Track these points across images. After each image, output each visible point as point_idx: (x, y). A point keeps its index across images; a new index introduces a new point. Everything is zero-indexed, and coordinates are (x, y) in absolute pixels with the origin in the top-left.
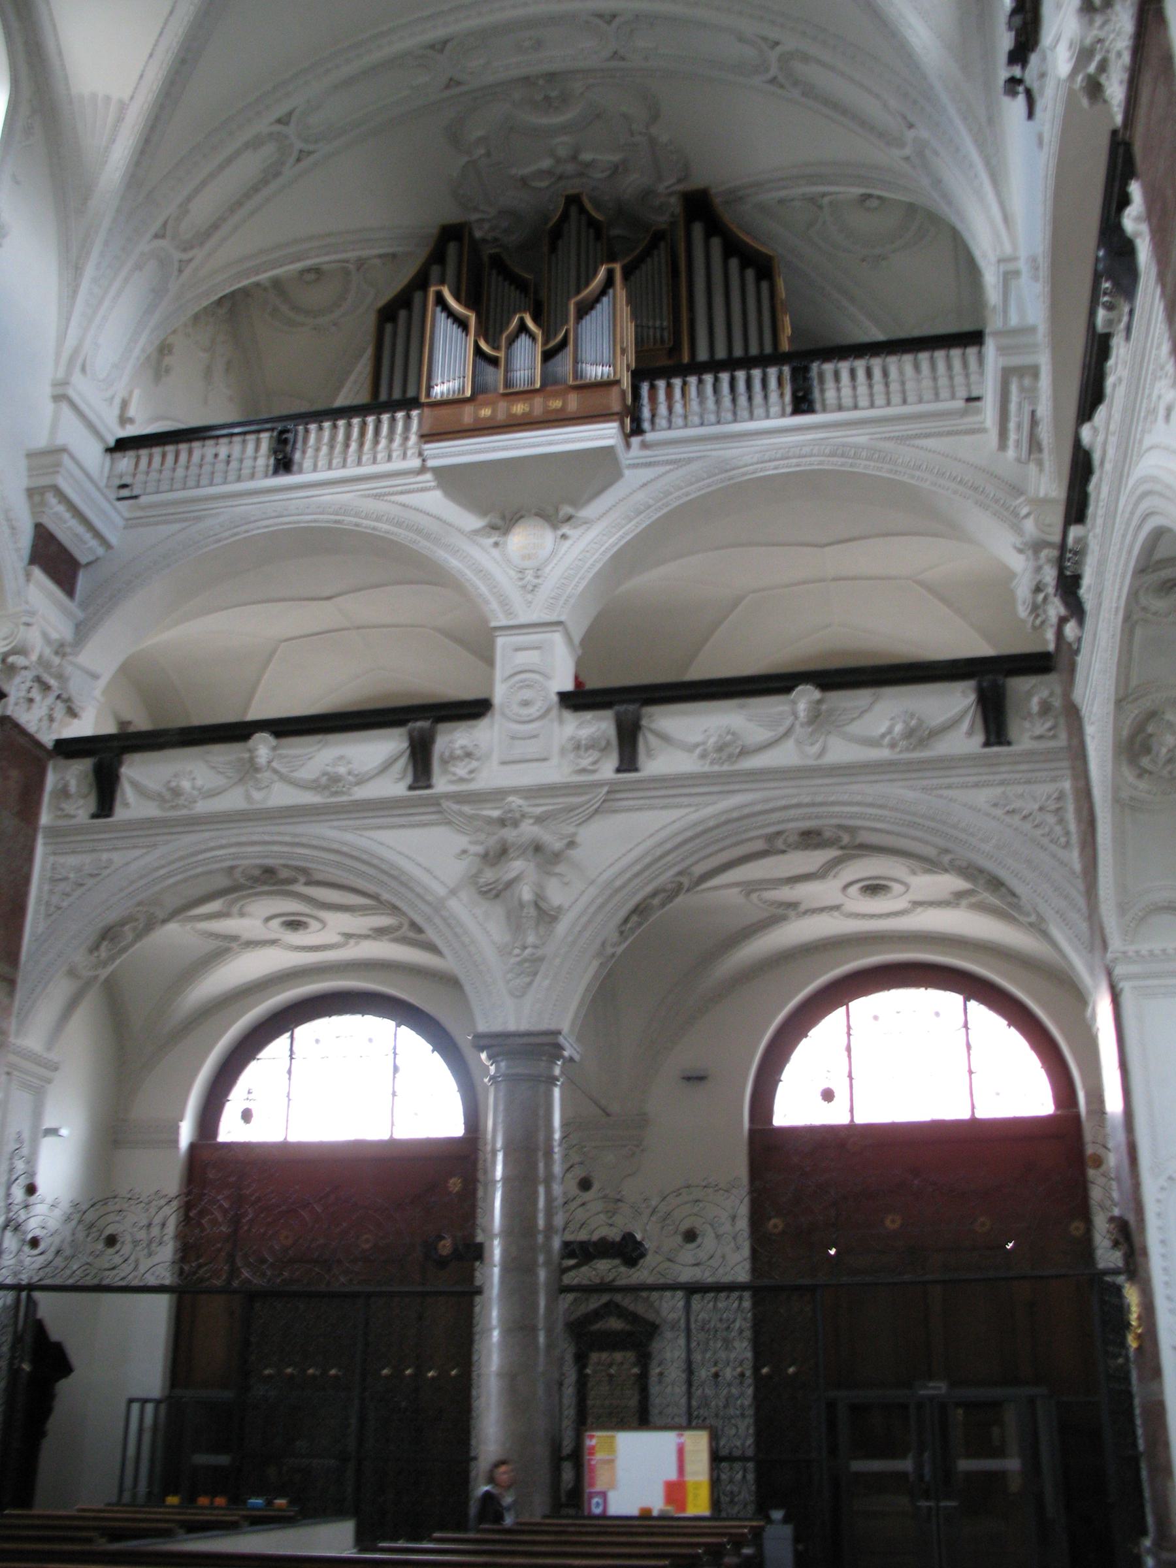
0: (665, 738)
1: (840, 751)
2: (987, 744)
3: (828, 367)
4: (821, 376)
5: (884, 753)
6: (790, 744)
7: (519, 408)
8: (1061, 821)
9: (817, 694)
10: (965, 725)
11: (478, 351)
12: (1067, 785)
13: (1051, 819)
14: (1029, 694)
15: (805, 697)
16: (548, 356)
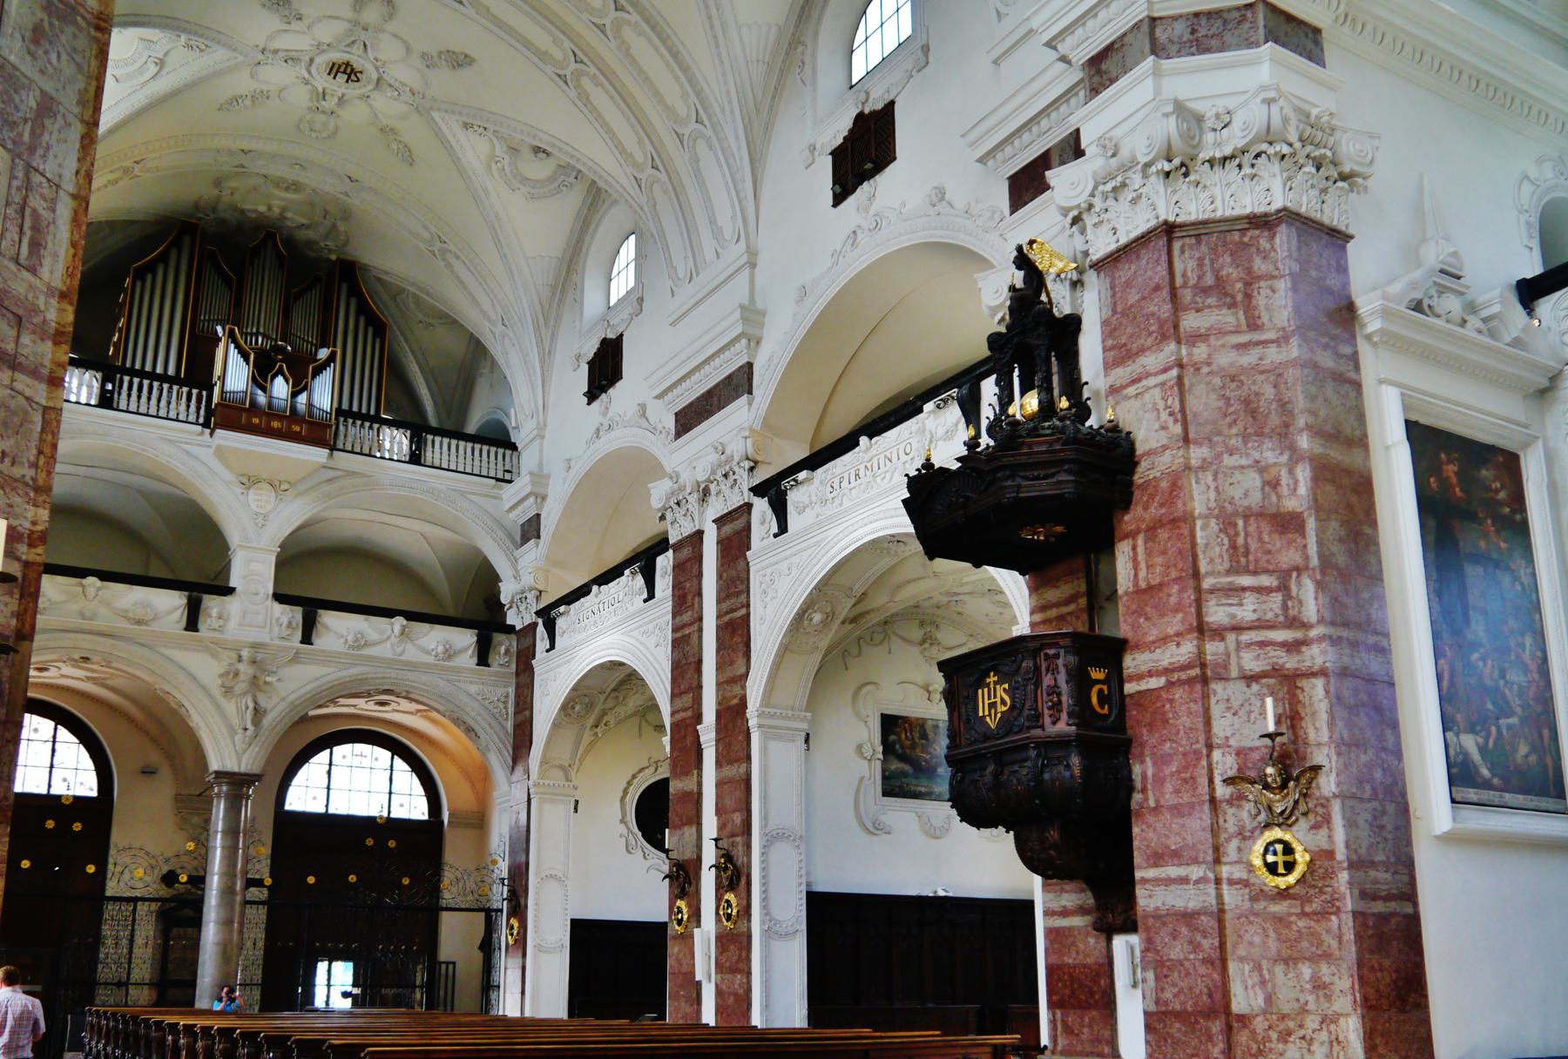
0: (327, 627)
1: (411, 653)
2: (478, 665)
3: (430, 437)
4: (426, 440)
5: (431, 659)
6: (388, 644)
7: (275, 424)
8: (506, 708)
9: (405, 622)
10: (470, 652)
11: (254, 380)
12: (511, 691)
13: (502, 706)
14: (500, 644)
15: (399, 621)
16: (295, 394)
